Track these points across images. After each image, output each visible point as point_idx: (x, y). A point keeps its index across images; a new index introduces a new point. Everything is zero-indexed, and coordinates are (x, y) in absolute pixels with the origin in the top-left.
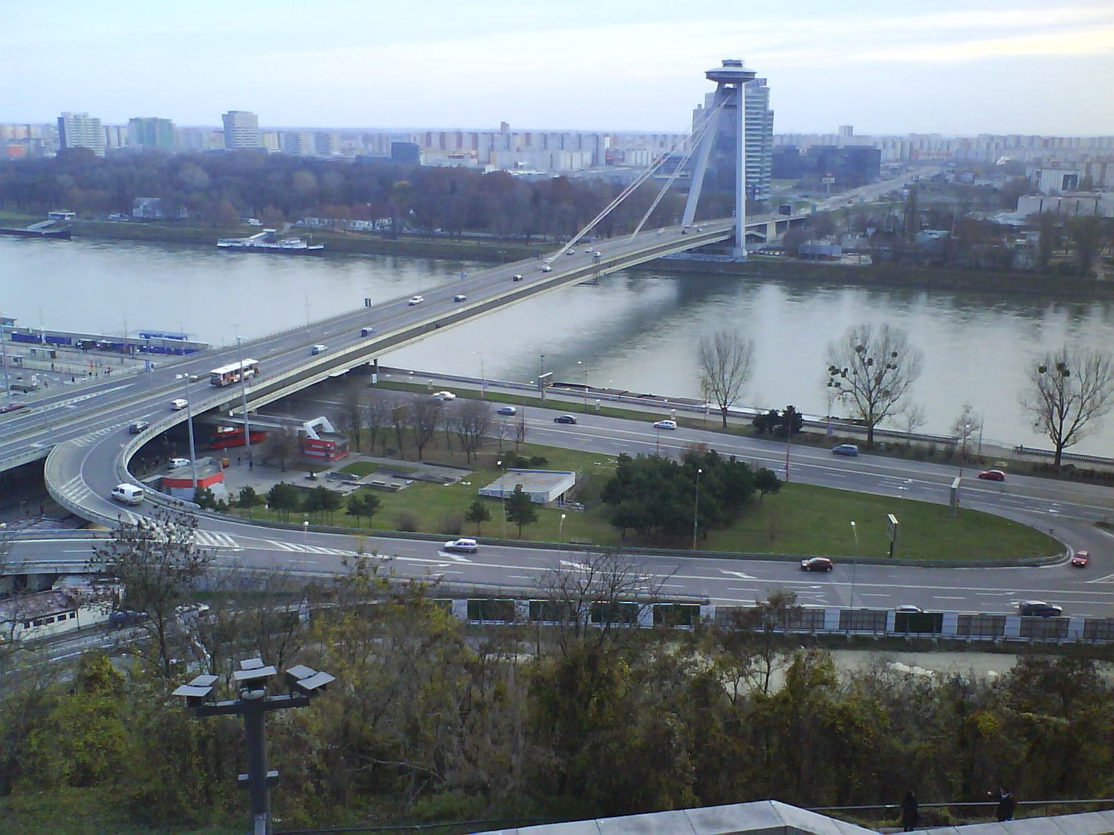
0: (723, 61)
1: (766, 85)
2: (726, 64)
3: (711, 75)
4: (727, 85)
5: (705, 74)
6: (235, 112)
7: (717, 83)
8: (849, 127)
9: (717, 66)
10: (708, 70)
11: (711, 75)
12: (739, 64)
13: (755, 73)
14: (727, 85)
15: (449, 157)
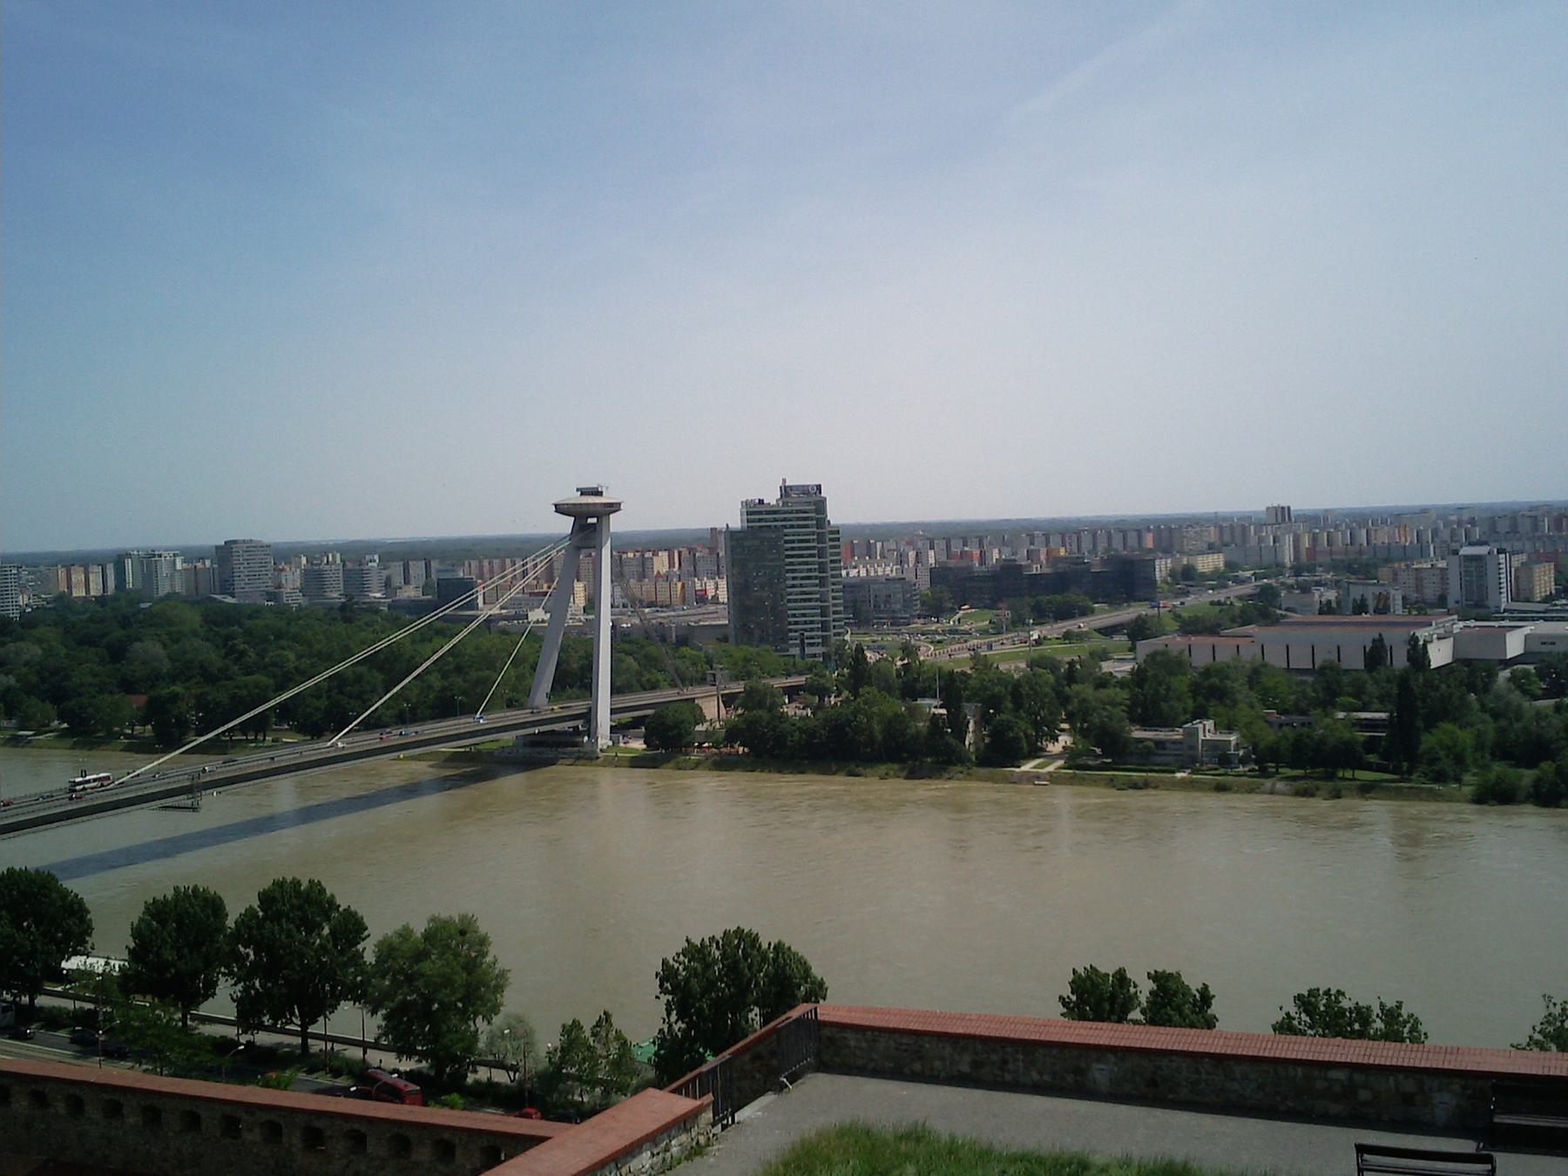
0: (578, 490)
1: (820, 493)
2: (584, 492)
3: (560, 509)
4: (590, 521)
5: (554, 507)
6: (234, 542)
7: (573, 518)
8: (1283, 508)
9: (575, 498)
10: (555, 501)
11: (560, 509)
12: (598, 493)
13: (620, 504)
14: (590, 521)
15: (531, 594)
